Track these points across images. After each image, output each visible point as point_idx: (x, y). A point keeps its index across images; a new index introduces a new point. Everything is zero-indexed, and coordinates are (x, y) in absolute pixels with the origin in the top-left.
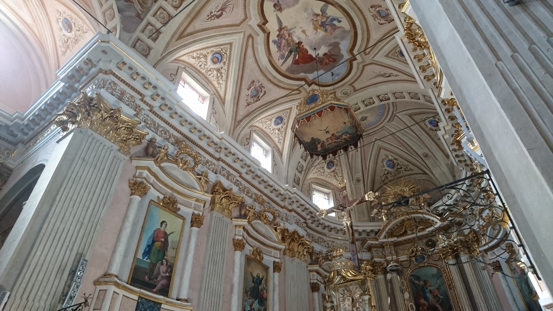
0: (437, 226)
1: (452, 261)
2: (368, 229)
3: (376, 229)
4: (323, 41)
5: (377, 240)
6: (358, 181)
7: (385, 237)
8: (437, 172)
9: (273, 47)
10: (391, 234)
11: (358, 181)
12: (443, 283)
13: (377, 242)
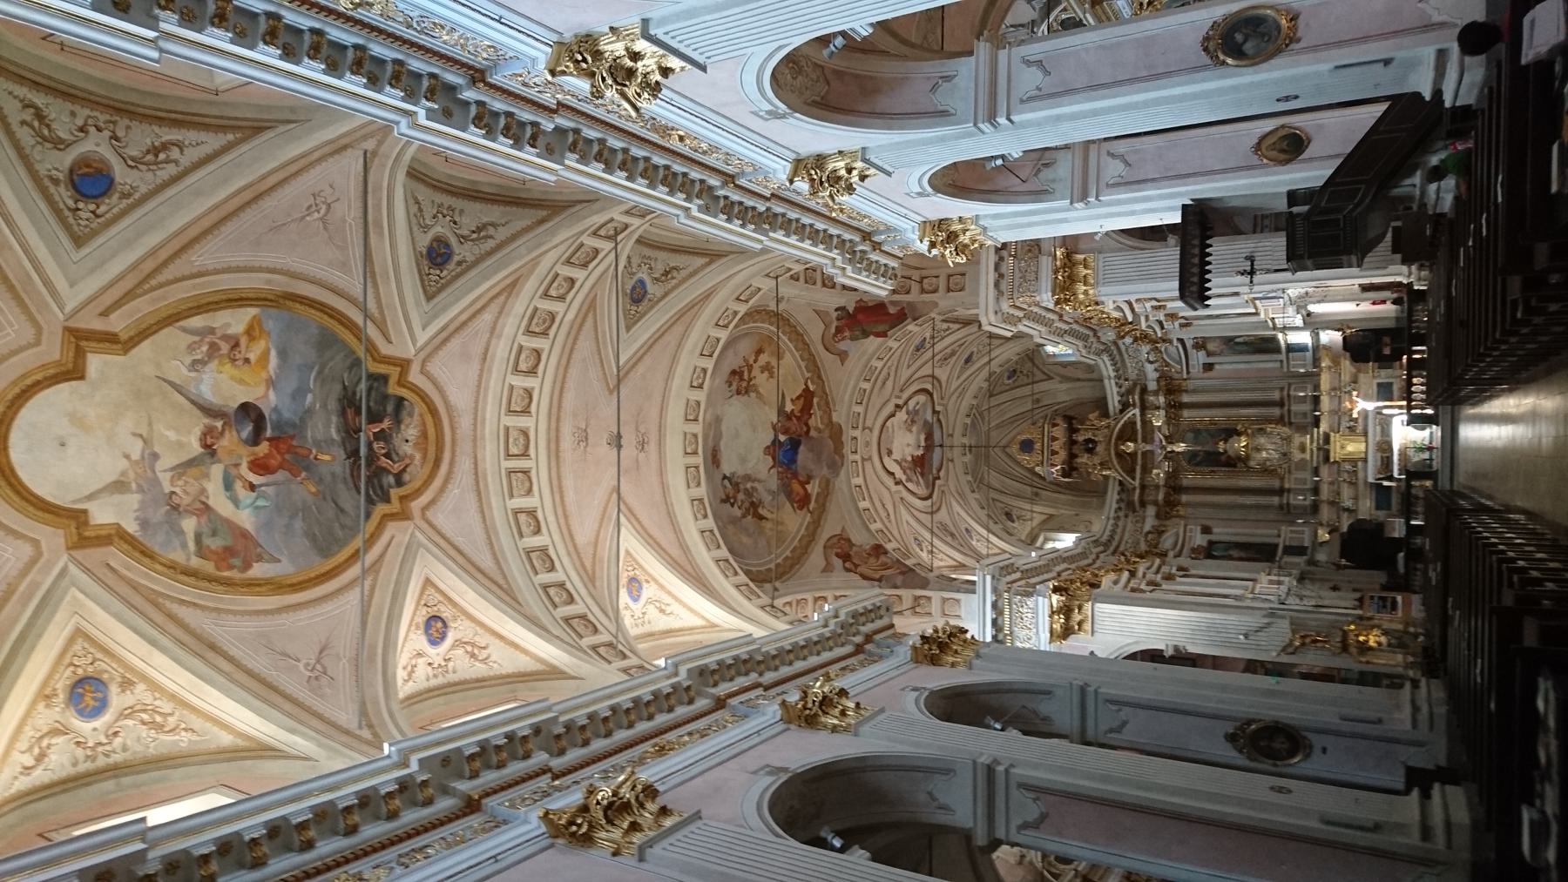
0: (1138, 414)
1: (1186, 413)
2: (1116, 497)
3: (1117, 488)
4: (919, 433)
5: (1134, 489)
6: (1037, 494)
7: (1134, 479)
8: (1063, 397)
9: (909, 485)
10: (1131, 472)
11: (1037, 494)
12: (1207, 430)
13: (1138, 491)
